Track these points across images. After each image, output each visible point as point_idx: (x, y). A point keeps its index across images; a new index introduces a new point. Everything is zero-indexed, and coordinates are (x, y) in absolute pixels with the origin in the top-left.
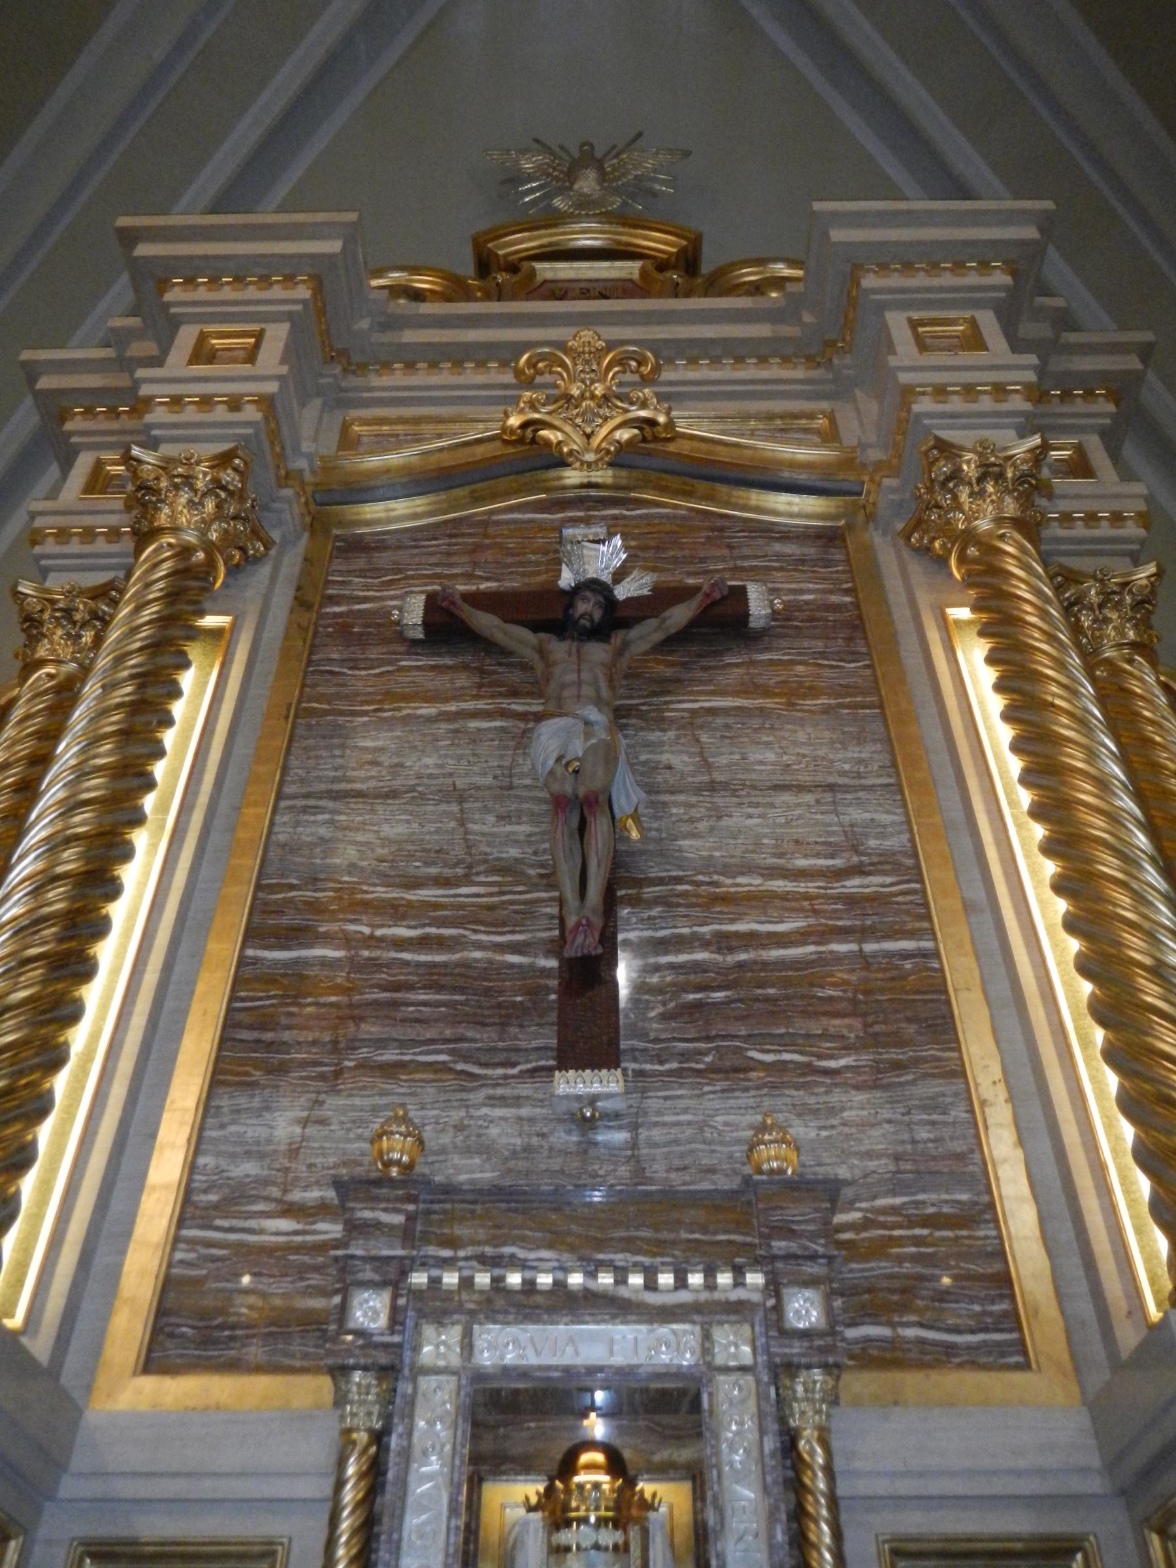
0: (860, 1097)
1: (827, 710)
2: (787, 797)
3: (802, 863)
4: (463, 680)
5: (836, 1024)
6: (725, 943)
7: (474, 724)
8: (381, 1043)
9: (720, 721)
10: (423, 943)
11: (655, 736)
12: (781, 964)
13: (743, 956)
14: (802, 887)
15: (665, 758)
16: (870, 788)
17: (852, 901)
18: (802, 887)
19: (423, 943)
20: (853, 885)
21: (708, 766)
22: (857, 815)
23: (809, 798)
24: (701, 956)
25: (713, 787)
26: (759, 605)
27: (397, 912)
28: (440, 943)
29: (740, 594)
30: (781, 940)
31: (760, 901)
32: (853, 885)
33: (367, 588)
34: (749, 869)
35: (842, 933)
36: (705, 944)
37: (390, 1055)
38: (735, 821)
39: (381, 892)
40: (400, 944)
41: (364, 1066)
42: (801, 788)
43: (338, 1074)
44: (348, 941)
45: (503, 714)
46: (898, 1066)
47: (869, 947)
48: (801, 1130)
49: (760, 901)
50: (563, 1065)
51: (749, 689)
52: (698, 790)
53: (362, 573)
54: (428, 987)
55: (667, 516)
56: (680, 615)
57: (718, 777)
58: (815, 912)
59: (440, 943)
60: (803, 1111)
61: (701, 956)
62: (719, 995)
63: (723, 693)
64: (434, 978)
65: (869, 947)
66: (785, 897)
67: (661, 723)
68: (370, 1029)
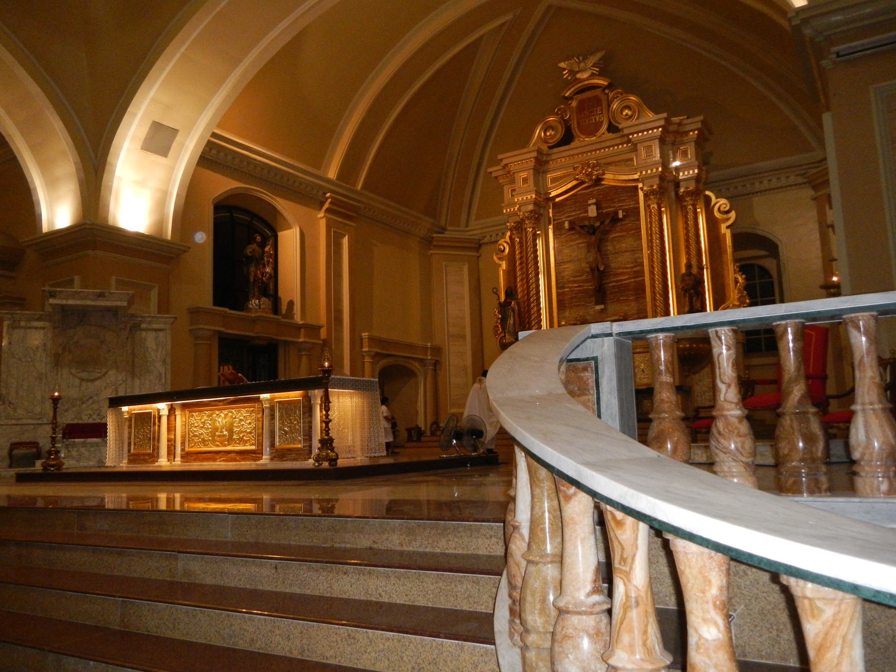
0: (633, 303)
1: (633, 234)
2: (627, 253)
3: (628, 266)
4: (577, 236)
5: (631, 293)
6: (617, 281)
7: (580, 245)
8: (576, 302)
9: (616, 239)
10: (579, 286)
11: (607, 244)
12: (625, 284)
13: (619, 283)
14: (629, 270)
15: (609, 248)
16: (639, 250)
17: (635, 272)
18: (629, 270)
19: (579, 286)
20: (635, 269)
21: (615, 249)
22: (637, 255)
23: (629, 253)
24: (614, 284)
25: (616, 253)
26: (621, 215)
27: (575, 282)
28: (582, 286)
29: (617, 213)
30: (625, 280)
31: (622, 274)
32: (635, 269)
33: (560, 216)
34: (621, 268)
35: (634, 278)
36: (615, 282)
37: (577, 304)
38: (619, 259)
39: (572, 279)
40: (575, 287)
41: (574, 306)
42: (629, 251)
43: (572, 307)
44: (569, 287)
45: (584, 242)
46: (639, 298)
47: (636, 280)
48: (626, 308)
49: (622, 274)
50: (597, 305)
51: (622, 231)
52: (613, 254)
53: (558, 213)
54: (581, 293)
55: (606, 188)
56: (607, 221)
57: (617, 251)
58: (629, 275)
59: (582, 286)
60: (626, 306)
61: (614, 284)
62: (616, 290)
63: (617, 232)
65: (636, 280)
66: (626, 272)
67: (607, 241)
68: (575, 300)
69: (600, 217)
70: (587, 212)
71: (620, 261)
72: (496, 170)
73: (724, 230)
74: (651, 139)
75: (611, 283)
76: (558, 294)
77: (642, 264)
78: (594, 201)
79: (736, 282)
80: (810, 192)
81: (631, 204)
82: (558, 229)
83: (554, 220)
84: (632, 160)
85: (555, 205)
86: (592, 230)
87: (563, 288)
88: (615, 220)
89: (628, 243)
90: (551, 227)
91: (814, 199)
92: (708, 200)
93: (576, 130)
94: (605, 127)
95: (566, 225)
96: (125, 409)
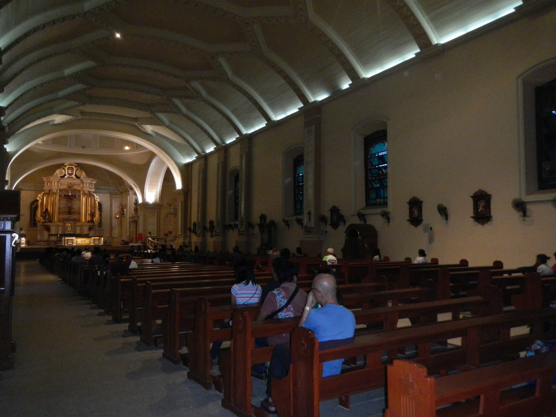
26: (77, 196)
49: (75, 209)
64: (65, 211)
69: (72, 196)
70: (68, 193)
71: (75, 206)
72: (45, 179)
73: (97, 202)
74: (88, 183)
75: (73, 211)
76: (59, 211)
77: (80, 208)
78: (70, 191)
79: (98, 213)
80: (108, 195)
81: (79, 194)
82: (60, 196)
83: (59, 193)
84: (80, 184)
85: (60, 190)
86: (70, 199)
87: (60, 210)
88: (76, 196)
89: (77, 202)
90: (58, 195)
91: (110, 197)
92: (94, 196)
93: (66, 174)
94: (74, 174)
95: (63, 196)
96: (66, 238)
